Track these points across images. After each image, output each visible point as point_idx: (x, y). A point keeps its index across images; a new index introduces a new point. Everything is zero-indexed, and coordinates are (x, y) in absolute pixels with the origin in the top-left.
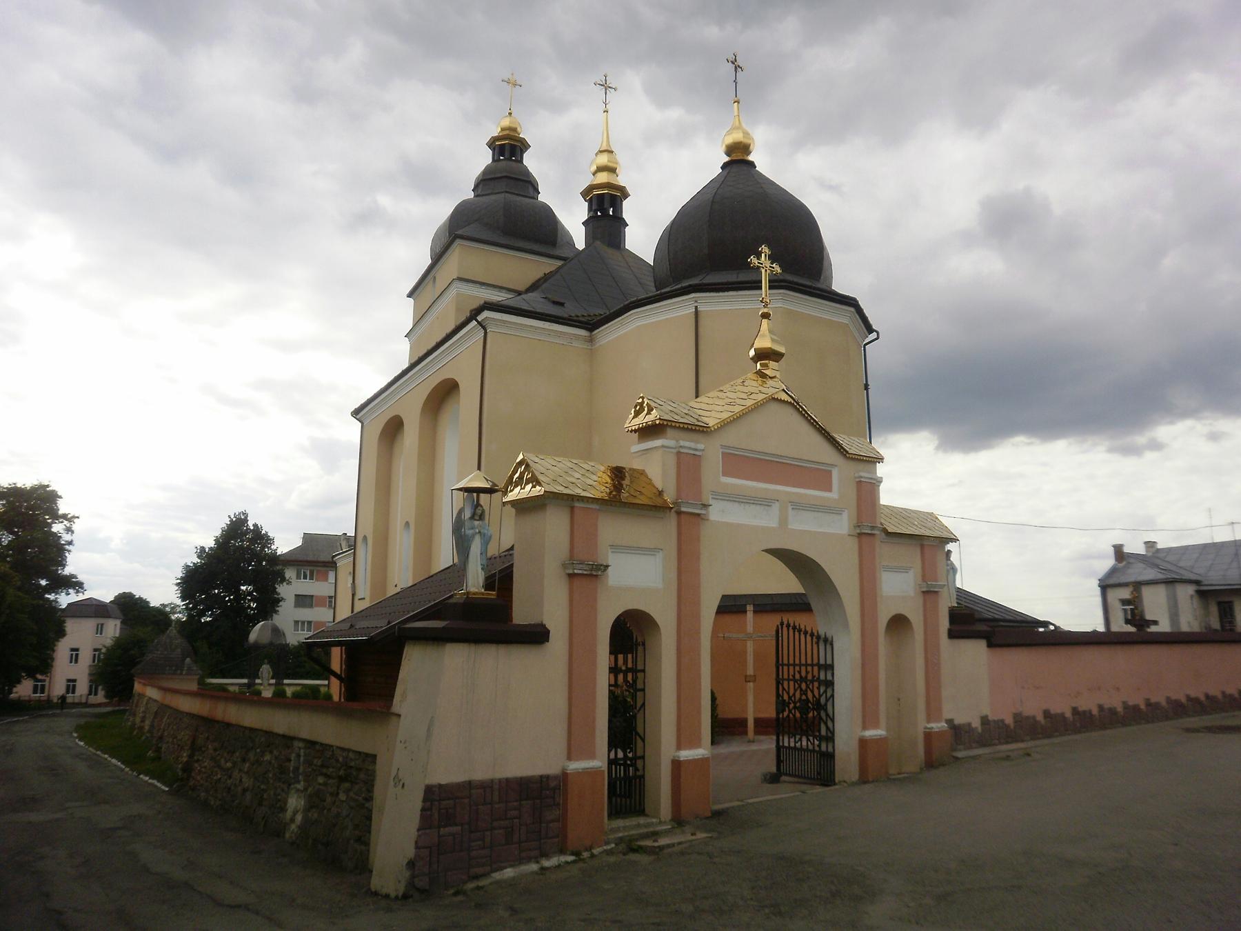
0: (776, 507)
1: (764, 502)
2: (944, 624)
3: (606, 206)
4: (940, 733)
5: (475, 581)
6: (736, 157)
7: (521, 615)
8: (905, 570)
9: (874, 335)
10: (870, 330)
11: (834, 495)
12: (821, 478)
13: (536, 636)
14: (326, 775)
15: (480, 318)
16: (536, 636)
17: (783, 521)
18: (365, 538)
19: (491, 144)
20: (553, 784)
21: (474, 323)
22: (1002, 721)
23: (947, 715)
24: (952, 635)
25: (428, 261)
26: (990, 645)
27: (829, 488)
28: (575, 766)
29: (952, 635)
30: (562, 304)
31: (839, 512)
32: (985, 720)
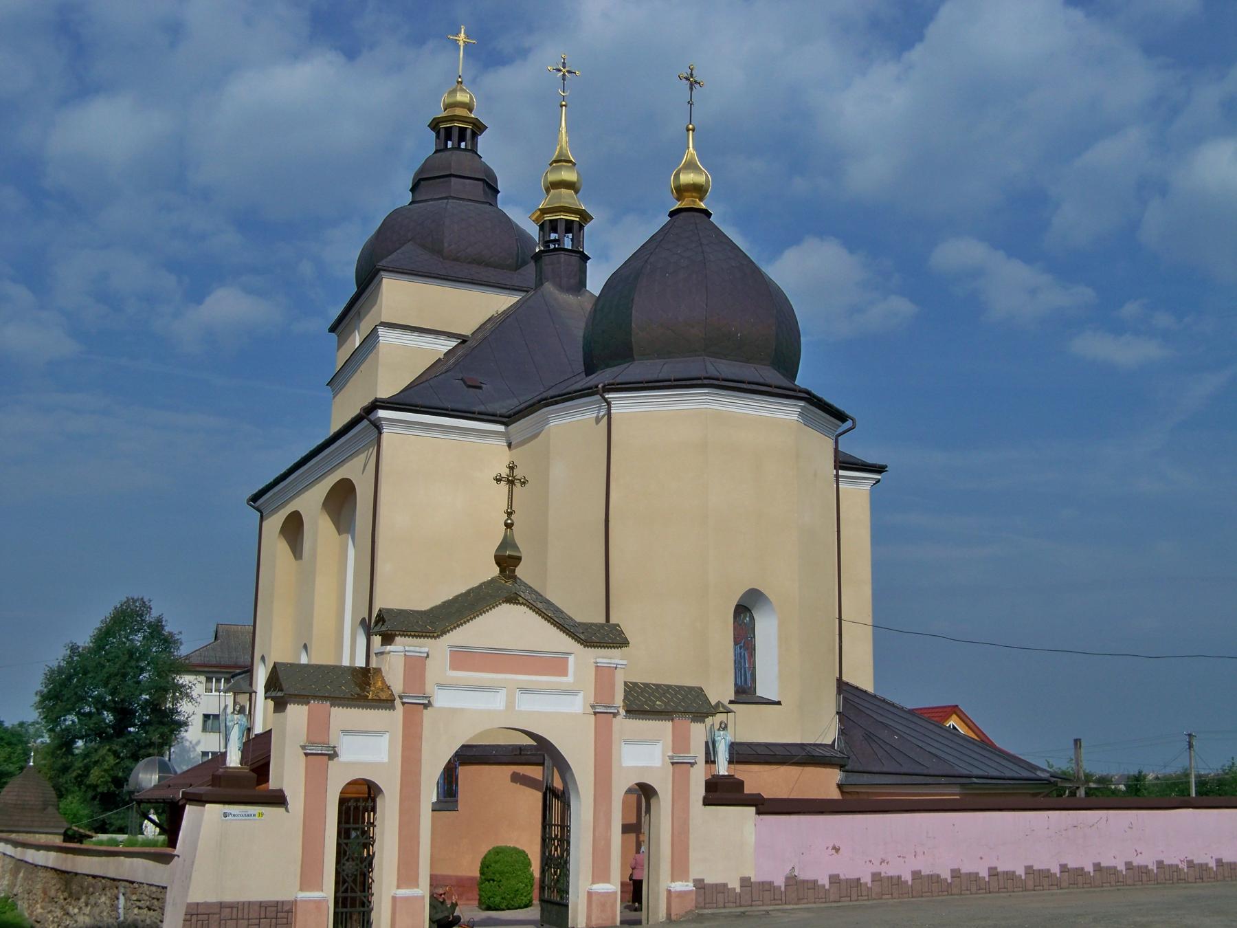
0: (503, 692)
1: (493, 689)
2: (698, 790)
3: (564, 228)
4: (682, 894)
5: (234, 759)
8: (654, 742)
9: (849, 424)
11: (570, 678)
12: (556, 664)
13: (278, 799)
14: (140, 908)
15: (372, 417)
16: (278, 799)
17: (510, 704)
18: (263, 658)
19: (435, 125)
20: (286, 908)
21: (365, 422)
22: (771, 883)
23: (696, 871)
24: (707, 802)
25: (354, 289)
26: (759, 813)
27: (565, 673)
28: (302, 895)
29: (707, 802)
30: (480, 388)
31: (573, 693)
32: (745, 882)
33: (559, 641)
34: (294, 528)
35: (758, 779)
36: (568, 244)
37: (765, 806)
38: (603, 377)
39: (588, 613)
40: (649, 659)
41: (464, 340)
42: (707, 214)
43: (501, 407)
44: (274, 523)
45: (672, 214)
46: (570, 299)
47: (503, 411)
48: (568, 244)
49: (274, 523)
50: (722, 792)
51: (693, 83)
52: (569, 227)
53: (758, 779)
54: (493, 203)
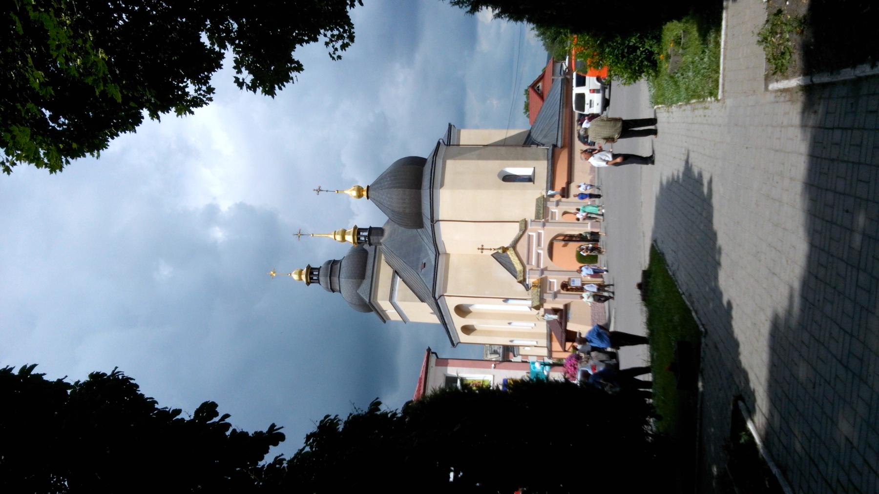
5: (556, 317)
6: (365, 193)
7: (561, 307)
10: (439, 143)
13: (567, 306)
18: (511, 341)
33: (525, 236)
34: (467, 330)
35: (561, 183)
36: (366, 234)
37: (570, 181)
38: (427, 223)
39: (514, 230)
40: (530, 213)
41: (396, 272)
42: (368, 187)
43: (432, 257)
44: (463, 338)
45: (368, 198)
46: (386, 234)
47: (434, 256)
48: (366, 234)
49: (463, 338)
50: (565, 193)
51: (319, 190)
52: (359, 233)
53: (561, 183)
54: (339, 262)
